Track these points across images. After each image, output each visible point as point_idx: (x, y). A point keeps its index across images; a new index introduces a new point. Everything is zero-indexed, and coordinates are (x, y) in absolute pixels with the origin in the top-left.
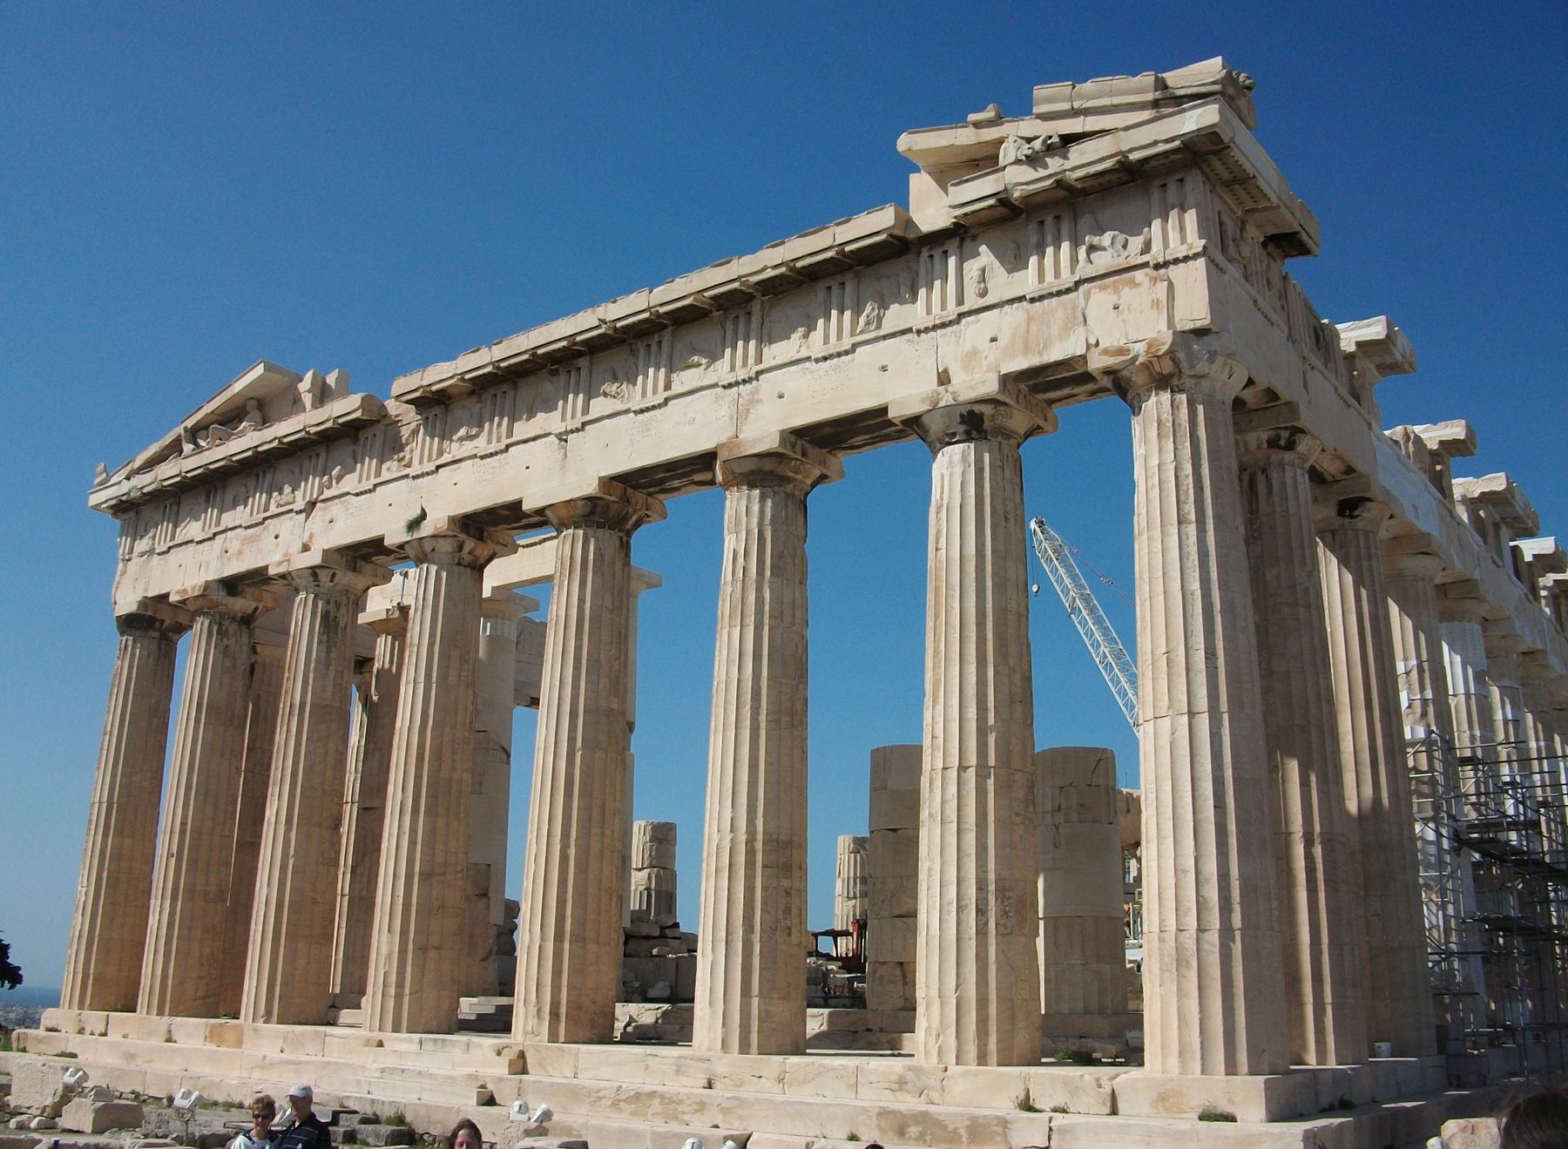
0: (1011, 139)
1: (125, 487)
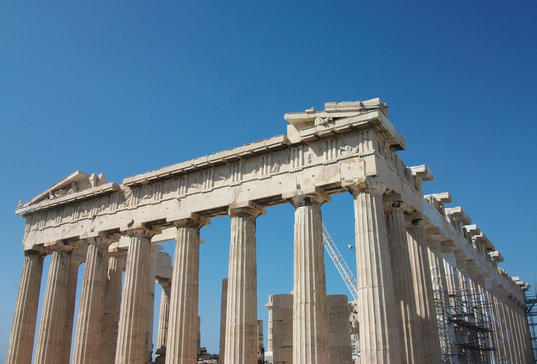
0: (318, 118)
1: (29, 208)
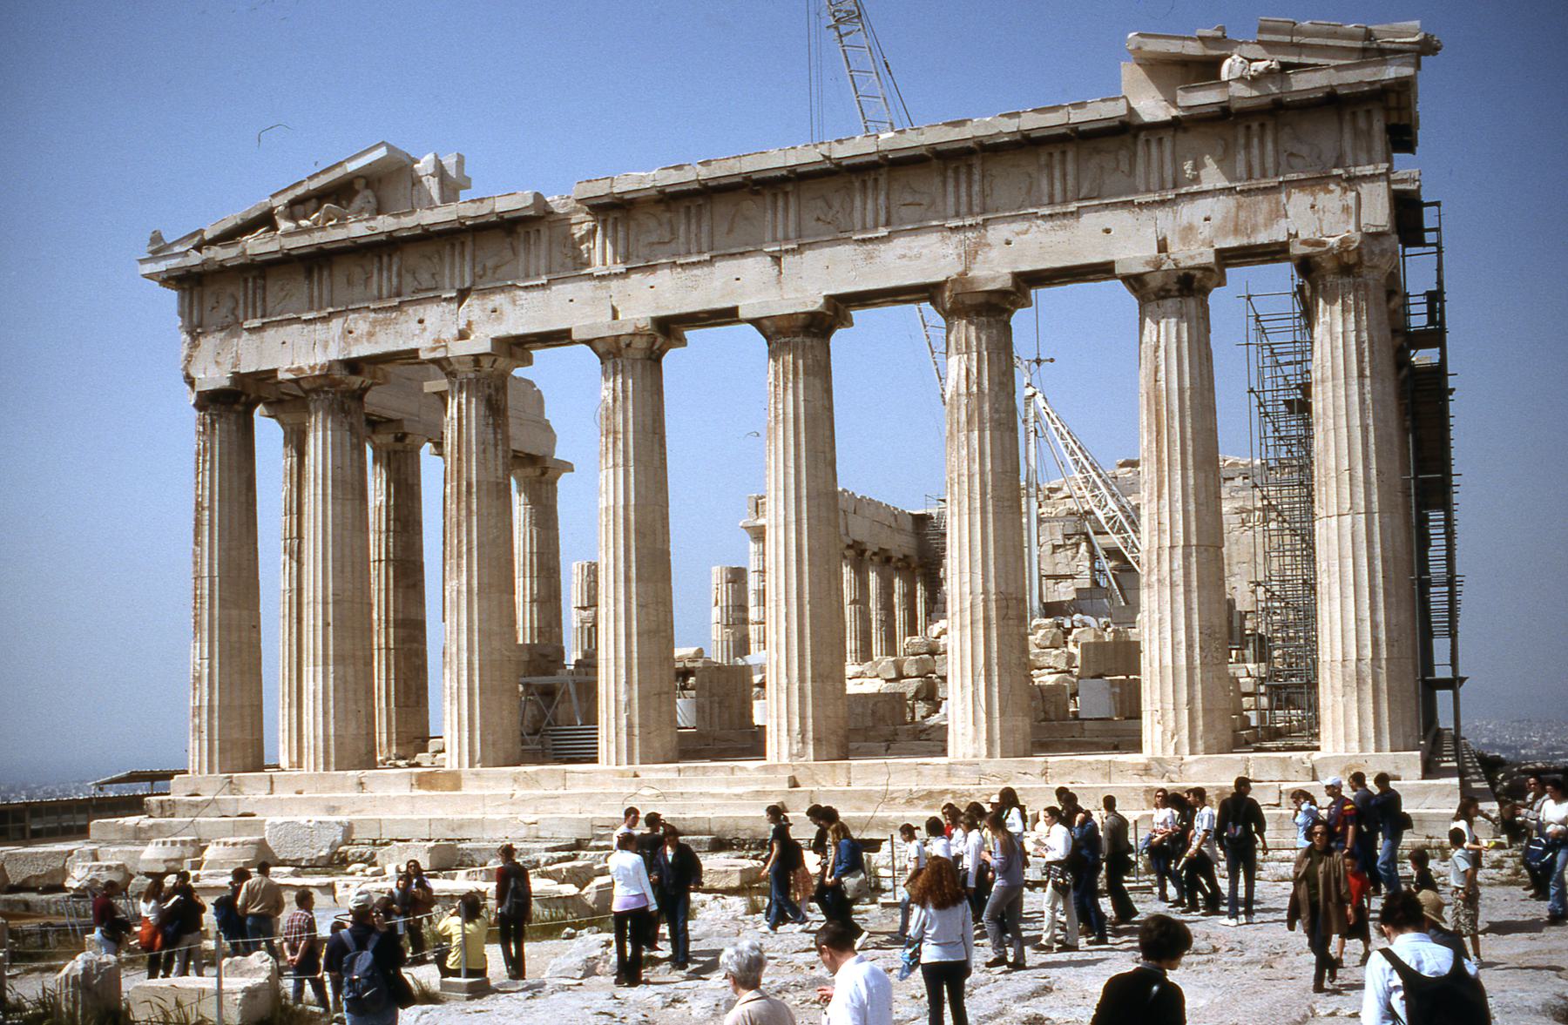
1: (195, 259)
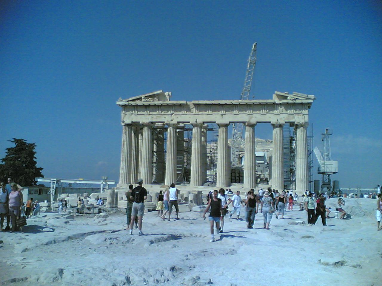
1: (127, 103)
